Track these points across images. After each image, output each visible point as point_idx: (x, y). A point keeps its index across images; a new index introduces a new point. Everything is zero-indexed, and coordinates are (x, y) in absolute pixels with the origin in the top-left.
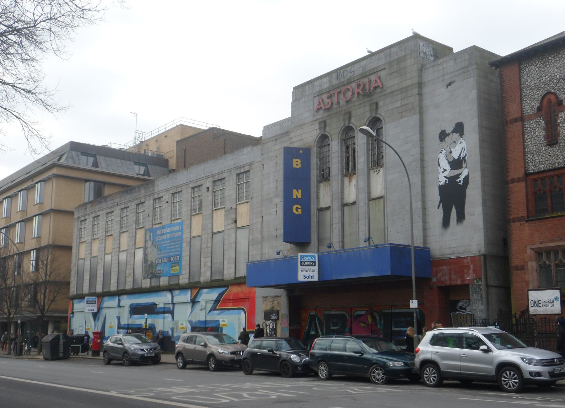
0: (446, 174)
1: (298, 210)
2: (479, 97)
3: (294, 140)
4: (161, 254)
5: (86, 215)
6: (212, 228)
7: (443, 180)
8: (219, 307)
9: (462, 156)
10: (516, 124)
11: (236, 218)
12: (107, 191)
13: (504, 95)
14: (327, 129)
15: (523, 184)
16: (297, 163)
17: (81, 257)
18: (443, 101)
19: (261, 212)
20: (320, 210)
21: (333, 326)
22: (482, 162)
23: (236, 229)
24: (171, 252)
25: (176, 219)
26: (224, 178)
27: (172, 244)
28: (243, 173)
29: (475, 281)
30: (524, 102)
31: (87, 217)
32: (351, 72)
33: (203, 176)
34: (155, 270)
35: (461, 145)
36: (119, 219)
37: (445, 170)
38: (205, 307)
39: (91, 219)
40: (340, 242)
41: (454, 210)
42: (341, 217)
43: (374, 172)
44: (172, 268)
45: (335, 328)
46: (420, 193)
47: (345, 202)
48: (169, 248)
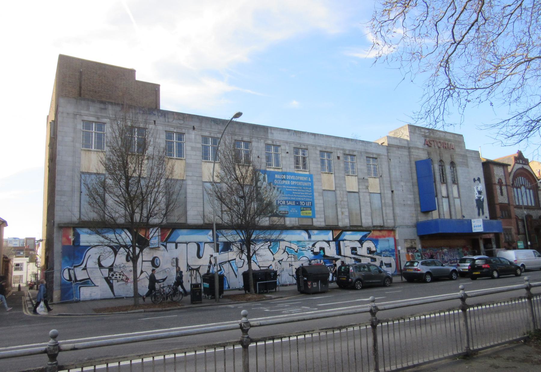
4: (283, 196)
7: (476, 198)
19: (391, 187)
24: (300, 197)
27: (299, 190)
34: (277, 210)
41: (481, 210)
44: (301, 211)
48: (295, 193)
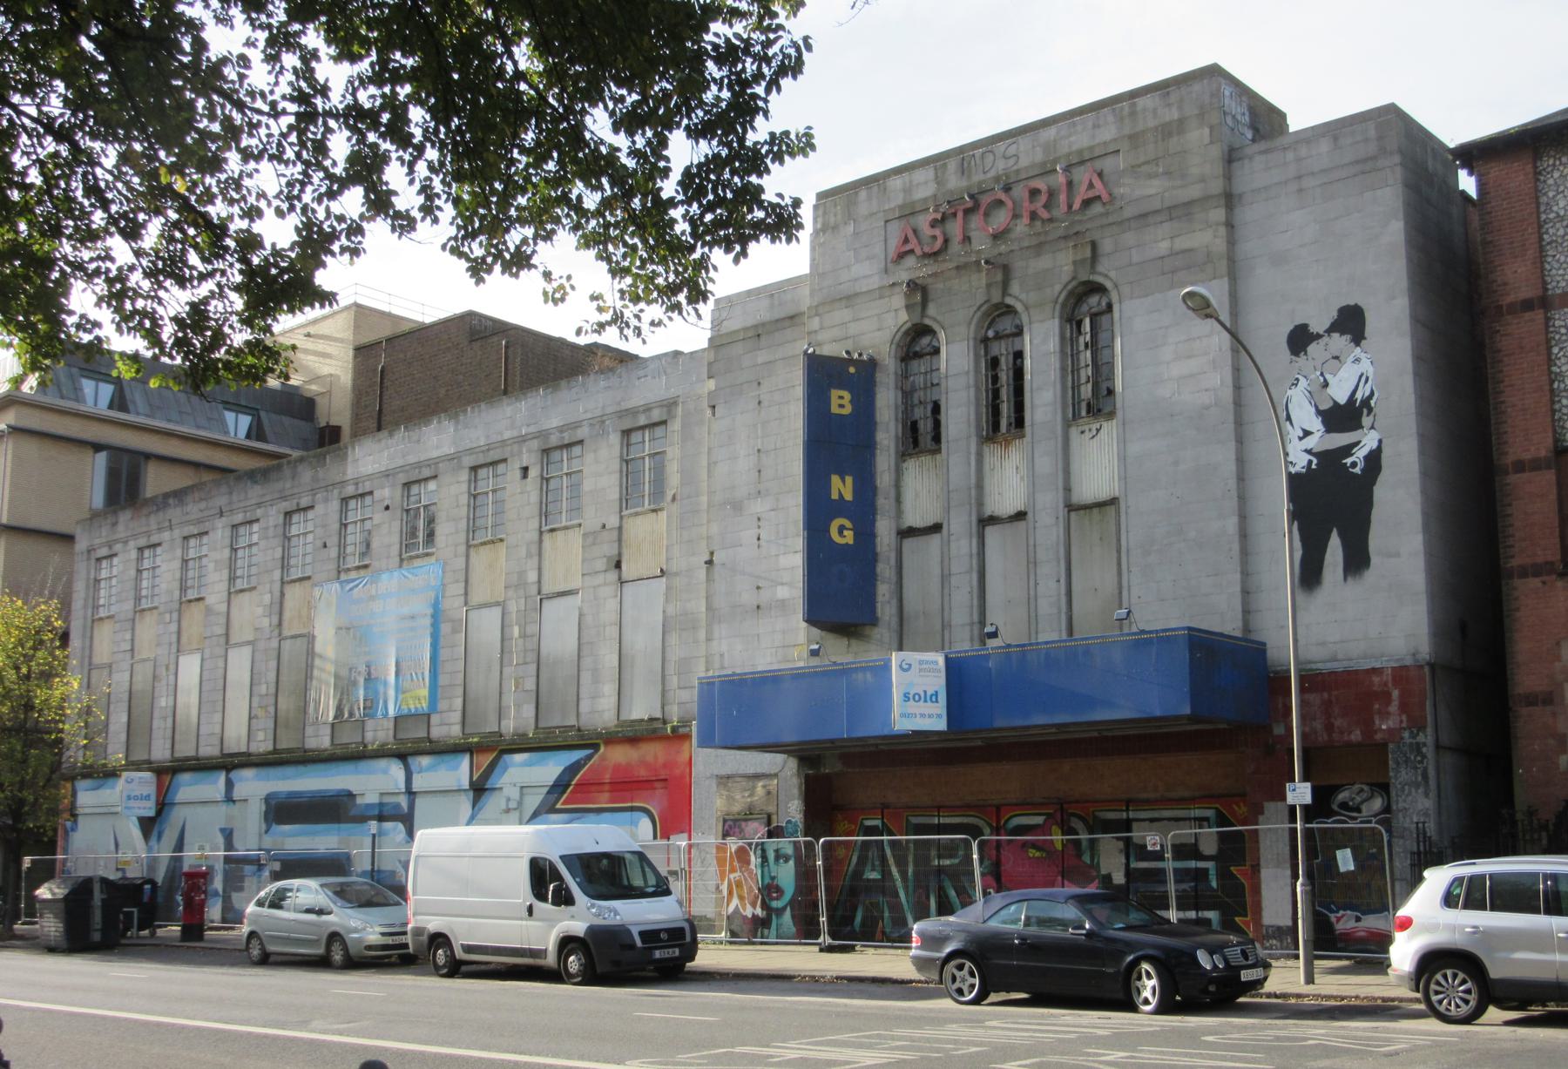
0: (1311, 442)
1: (846, 533)
2: (1410, 242)
3: (820, 337)
5: (117, 541)
6: (539, 582)
7: (1300, 461)
8: (565, 803)
9: (1359, 396)
10: (1528, 315)
11: (620, 554)
12: (155, 481)
13: (1489, 238)
14: (932, 310)
15: (1549, 476)
16: (841, 402)
17: (97, 660)
18: (1301, 246)
20: (907, 533)
21: (939, 858)
22: (1421, 414)
23: (622, 582)
25: (417, 557)
26: (581, 442)
28: (642, 428)
29: (1406, 734)
30: (1550, 259)
31: (118, 547)
32: (1005, 157)
33: (507, 435)
35: (1355, 366)
36: (227, 552)
37: (1307, 433)
38: (520, 803)
39: (134, 554)
40: (972, 624)
42: (978, 554)
43: (1082, 432)
45: (947, 862)
46: (1234, 493)
47: (988, 512)
